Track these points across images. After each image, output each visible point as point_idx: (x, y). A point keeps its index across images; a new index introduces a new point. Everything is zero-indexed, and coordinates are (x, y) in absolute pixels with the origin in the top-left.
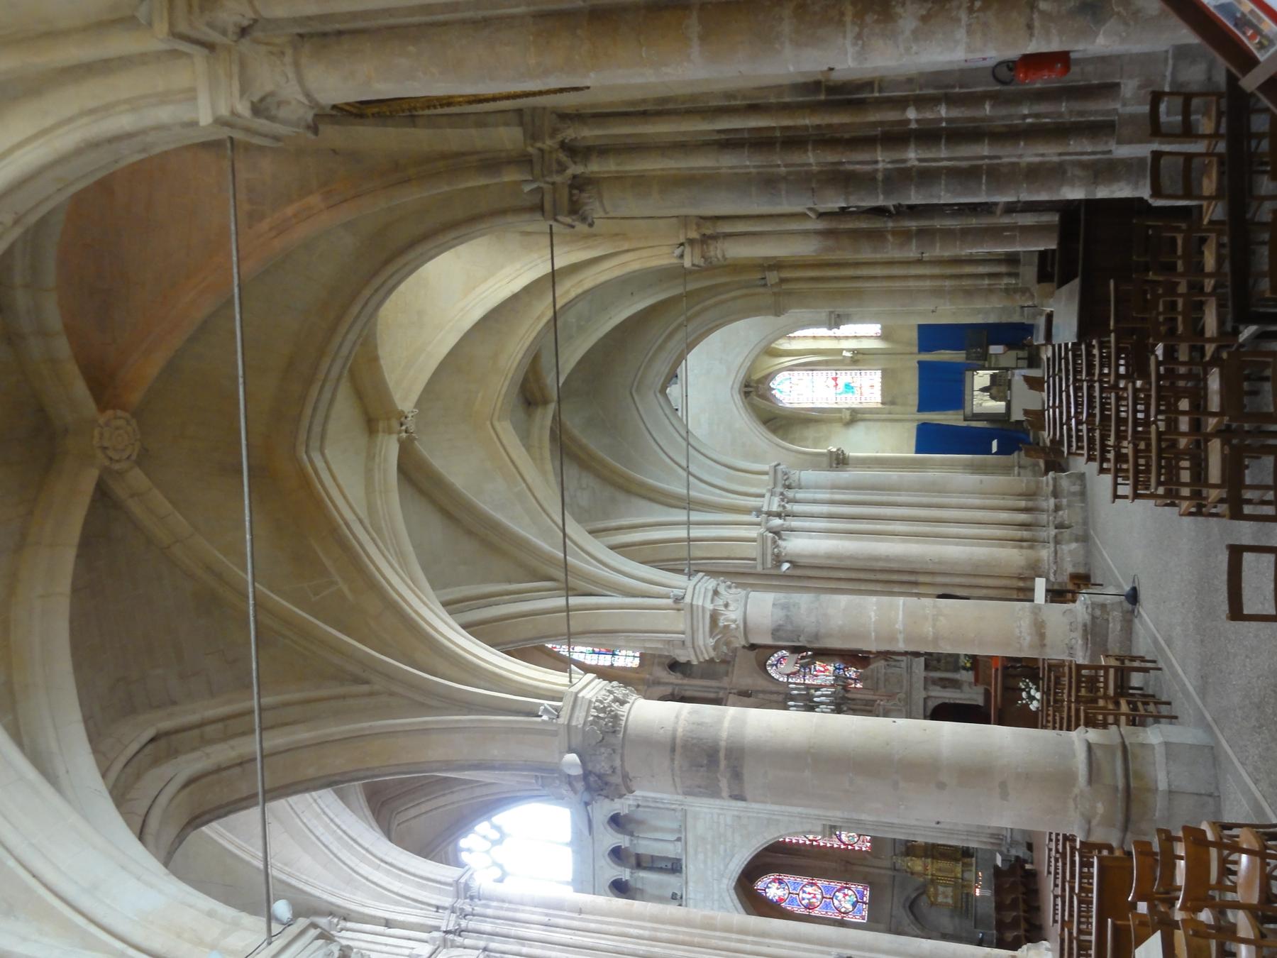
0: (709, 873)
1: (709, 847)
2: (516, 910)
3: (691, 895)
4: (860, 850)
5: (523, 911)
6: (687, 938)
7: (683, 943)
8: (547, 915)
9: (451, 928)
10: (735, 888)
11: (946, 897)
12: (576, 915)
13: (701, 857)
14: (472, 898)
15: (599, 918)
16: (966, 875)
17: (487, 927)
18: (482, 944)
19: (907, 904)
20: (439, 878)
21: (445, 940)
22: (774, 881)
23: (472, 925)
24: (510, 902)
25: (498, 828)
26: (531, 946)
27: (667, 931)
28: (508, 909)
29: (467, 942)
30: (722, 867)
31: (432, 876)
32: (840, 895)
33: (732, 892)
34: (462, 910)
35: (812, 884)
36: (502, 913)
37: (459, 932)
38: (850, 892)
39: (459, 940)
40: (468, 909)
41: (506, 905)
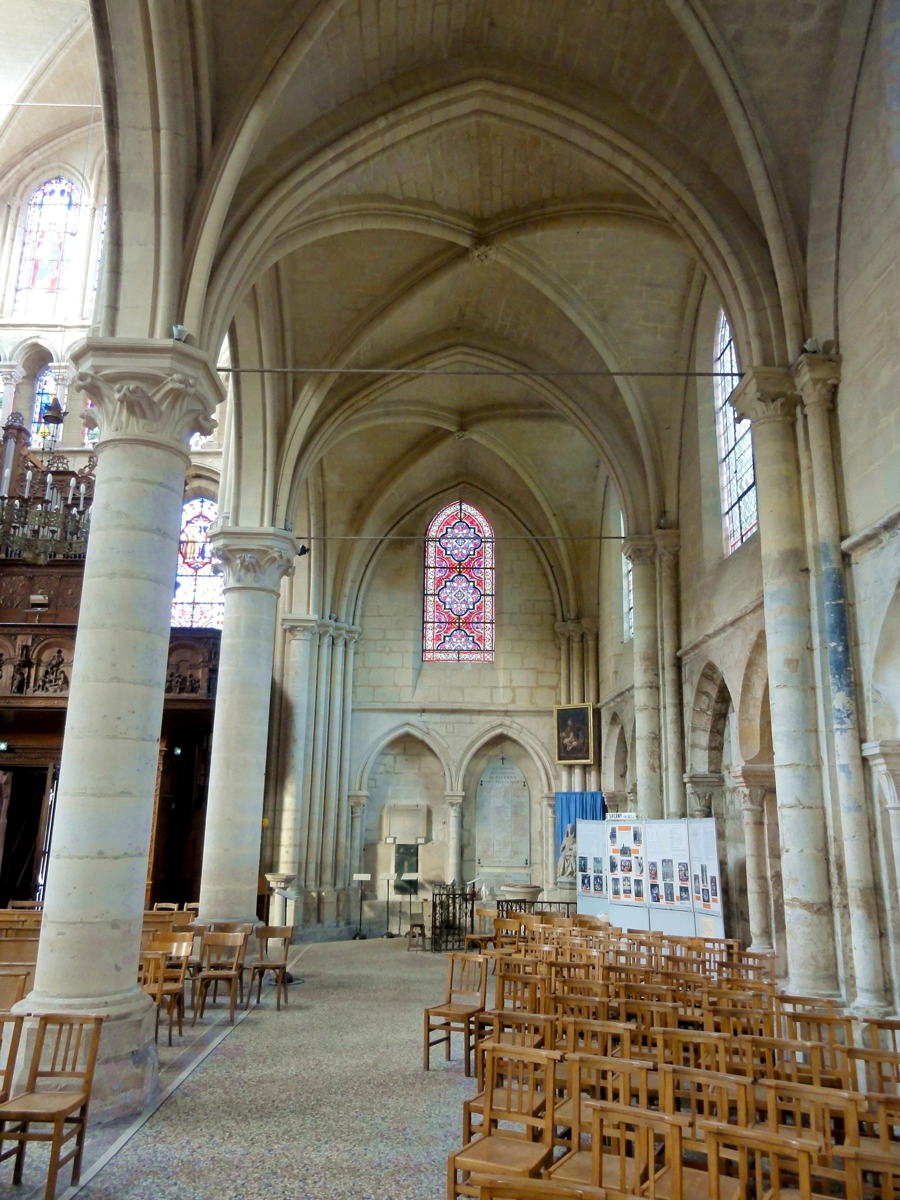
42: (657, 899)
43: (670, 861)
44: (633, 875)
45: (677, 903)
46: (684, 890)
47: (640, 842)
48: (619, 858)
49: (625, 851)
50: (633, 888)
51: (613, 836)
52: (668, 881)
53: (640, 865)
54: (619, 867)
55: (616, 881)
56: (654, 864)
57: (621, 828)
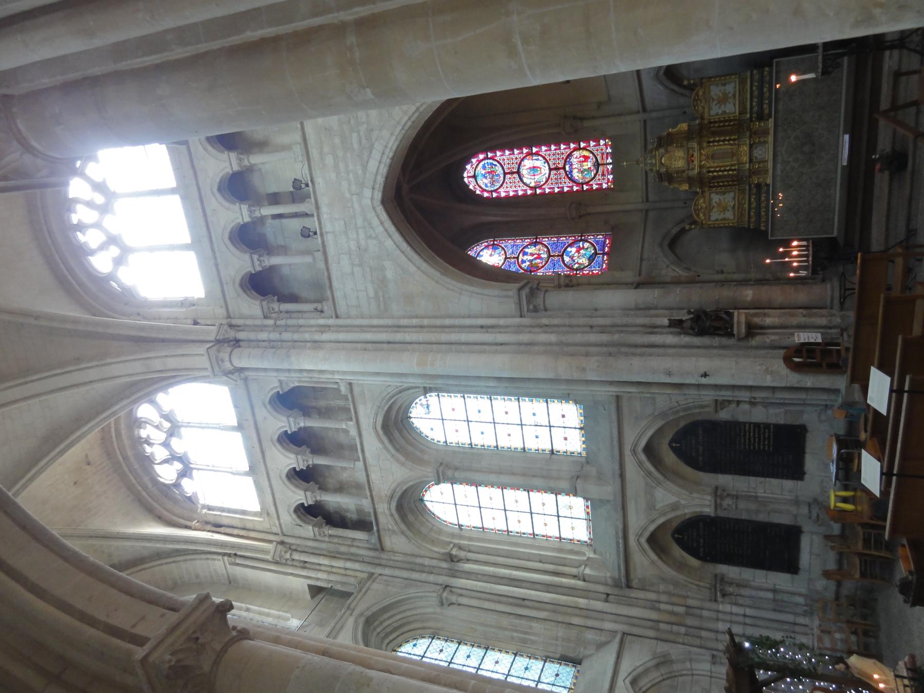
0: (345, 184)
1: (337, 140)
3: (328, 227)
4: (600, 189)
10: (383, 202)
11: (725, 209)
13: (329, 160)
16: (758, 153)
19: (666, 243)
22: (487, 247)
25: (100, 187)
30: (360, 172)
32: (573, 250)
33: (380, 209)
35: (535, 244)
38: (586, 245)
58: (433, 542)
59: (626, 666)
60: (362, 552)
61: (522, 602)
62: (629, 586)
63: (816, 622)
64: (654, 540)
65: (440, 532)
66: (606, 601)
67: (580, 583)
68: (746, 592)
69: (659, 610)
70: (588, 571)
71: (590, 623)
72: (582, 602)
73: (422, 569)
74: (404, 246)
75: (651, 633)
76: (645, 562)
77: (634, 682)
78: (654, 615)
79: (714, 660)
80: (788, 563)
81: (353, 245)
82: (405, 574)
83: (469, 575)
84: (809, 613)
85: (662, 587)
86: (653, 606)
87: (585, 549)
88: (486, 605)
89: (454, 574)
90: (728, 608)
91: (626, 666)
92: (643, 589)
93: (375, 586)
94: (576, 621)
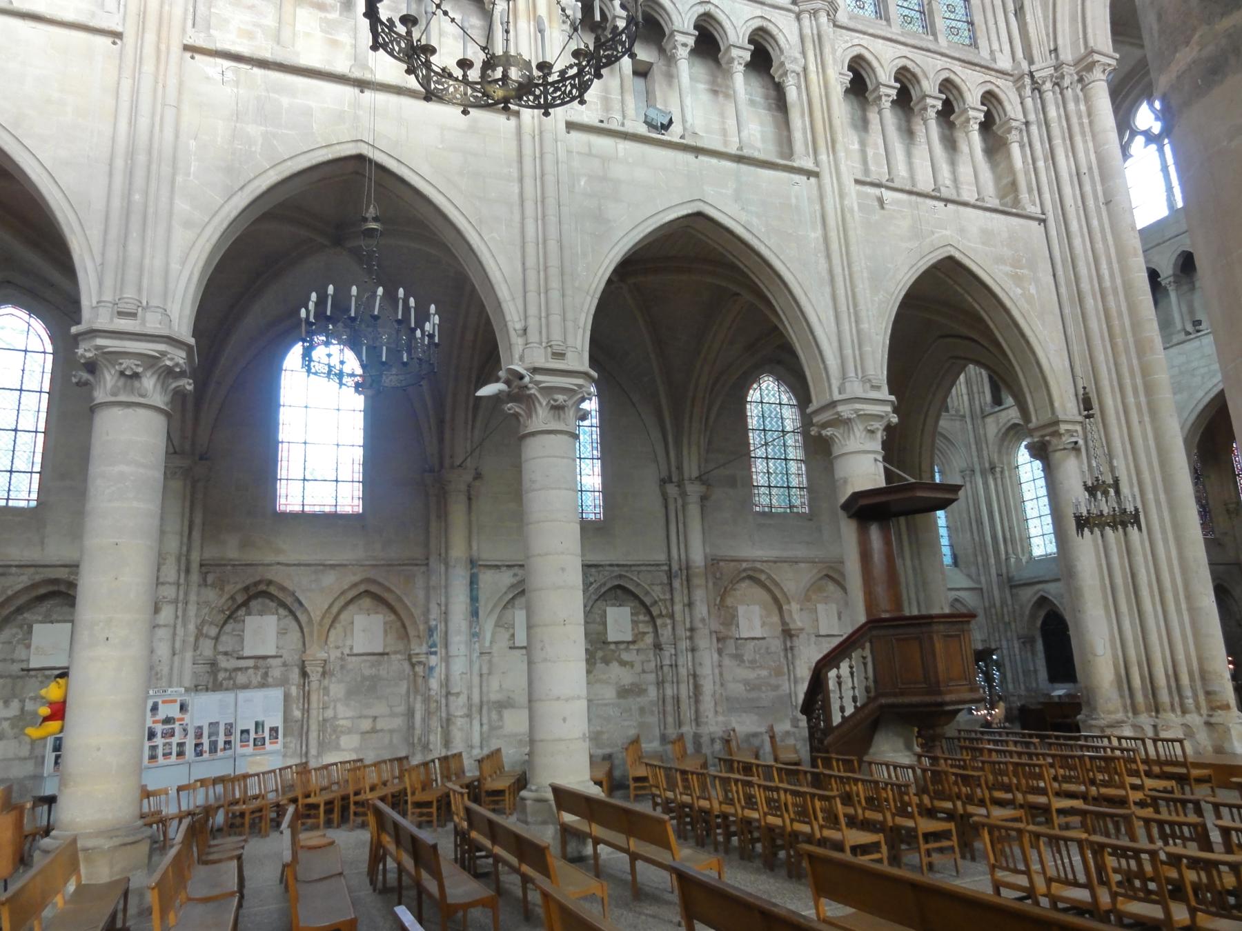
2: (1083, 134)
5: (1085, 142)
6: (1117, 330)
7: (1110, 328)
8: (1090, 169)
9: (1037, 75)
12: (1101, 199)
14: (1081, 80)
15: (1107, 226)
17: (1052, 113)
18: (1032, 117)
20: (1090, 30)
21: (1021, 77)
23: (1049, 96)
24: (1091, 123)
26: (1047, 169)
27: (1118, 306)
28: (1081, 125)
29: (1029, 101)
31: (1089, 20)
34: (1062, 77)
36: (1074, 120)
37: (1037, 88)
39: (1028, 91)
40: (1066, 82)
41: (1086, 121)
42: (199, 754)
43: (218, 723)
44: (175, 740)
45: (220, 754)
46: (227, 743)
47: (186, 711)
48: (159, 728)
49: (168, 720)
50: (175, 750)
51: (155, 708)
52: (213, 738)
53: (185, 730)
54: (159, 735)
55: (154, 748)
56: (200, 728)
57: (164, 702)
58: (1000, 452)
59: (962, 594)
60: (977, 403)
61: (980, 523)
62: (1011, 587)
63: (1023, 693)
64: (1043, 601)
65: (1008, 454)
66: (998, 575)
67: (1003, 557)
68: (1029, 654)
69: (1002, 607)
70: (1013, 560)
71: (981, 568)
72: (992, 561)
73: (979, 450)
74: (1201, 407)
75: (987, 604)
76: (1028, 596)
77: (956, 600)
78: (998, 604)
79: (984, 641)
80: (1054, 678)
81: (1195, 364)
82: (972, 440)
83: (986, 484)
84: (1027, 689)
85: (1017, 607)
86: (1003, 603)
87: (1027, 555)
88: (971, 501)
89: (983, 473)
90: (1016, 645)
91: (962, 594)
92: (1012, 596)
93: (958, 423)
94: (980, 559)
